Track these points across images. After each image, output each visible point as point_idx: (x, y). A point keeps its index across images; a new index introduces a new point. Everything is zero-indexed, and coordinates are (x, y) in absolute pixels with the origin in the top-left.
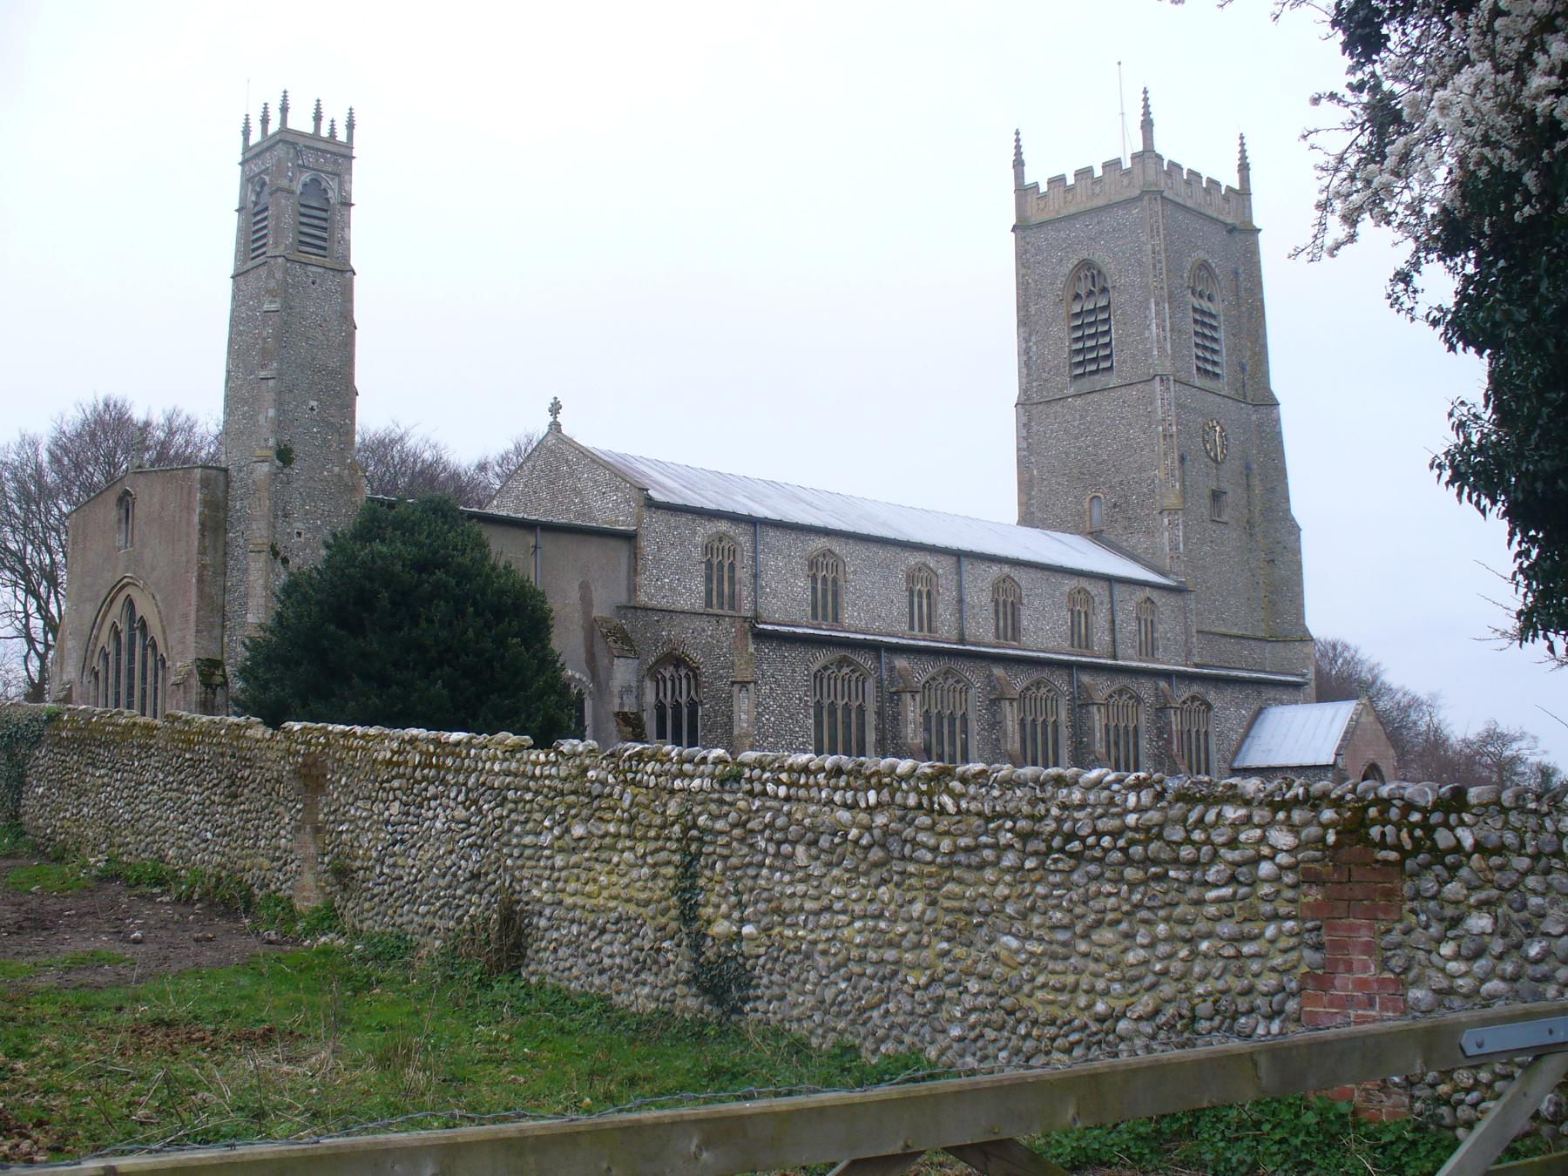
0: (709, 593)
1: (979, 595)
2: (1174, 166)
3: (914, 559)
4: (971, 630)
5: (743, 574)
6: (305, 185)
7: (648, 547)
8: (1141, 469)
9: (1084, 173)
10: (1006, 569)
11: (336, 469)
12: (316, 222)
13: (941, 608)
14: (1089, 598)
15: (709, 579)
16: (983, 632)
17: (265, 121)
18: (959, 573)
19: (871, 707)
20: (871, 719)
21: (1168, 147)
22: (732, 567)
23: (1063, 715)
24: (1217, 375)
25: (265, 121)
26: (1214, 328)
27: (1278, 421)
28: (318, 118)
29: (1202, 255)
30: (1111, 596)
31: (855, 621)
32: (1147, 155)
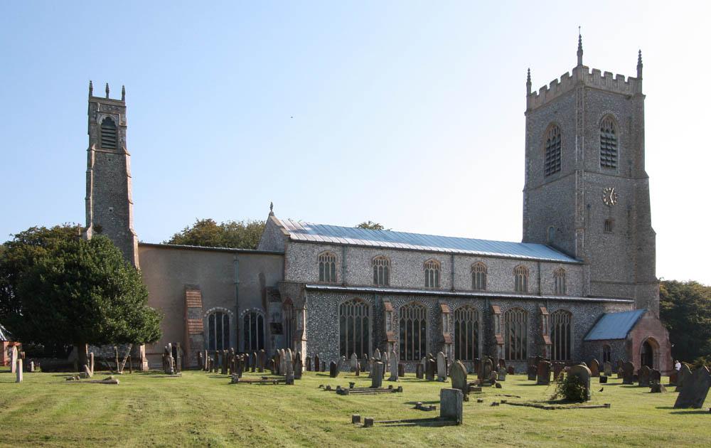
0: (321, 275)
4: (458, 285)
5: (338, 267)
6: (103, 120)
7: (290, 258)
8: (569, 213)
9: (554, 83)
10: (479, 259)
11: (123, 234)
12: (109, 135)
13: (442, 277)
14: (526, 272)
15: (321, 270)
16: (465, 284)
19: (371, 318)
20: (371, 323)
21: (590, 62)
22: (333, 265)
23: (481, 319)
24: (615, 167)
26: (615, 146)
27: (648, 185)
28: (107, 91)
29: (609, 111)
30: (539, 267)
32: (580, 68)
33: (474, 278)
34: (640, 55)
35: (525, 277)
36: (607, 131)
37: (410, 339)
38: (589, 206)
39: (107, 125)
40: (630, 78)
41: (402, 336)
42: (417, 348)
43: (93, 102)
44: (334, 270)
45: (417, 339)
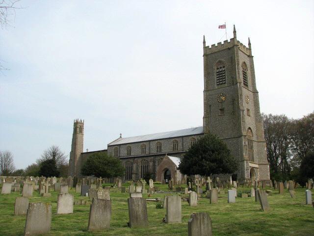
1: (154, 146)
2: (213, 46)
3: (141, 144)
10: (159, 141)
21: (209, 44)
31: (133, 154)
34: (234, 27)
36: (221, 68)
38: (210, 106)
40: (231, 39)
43: (75, 123)
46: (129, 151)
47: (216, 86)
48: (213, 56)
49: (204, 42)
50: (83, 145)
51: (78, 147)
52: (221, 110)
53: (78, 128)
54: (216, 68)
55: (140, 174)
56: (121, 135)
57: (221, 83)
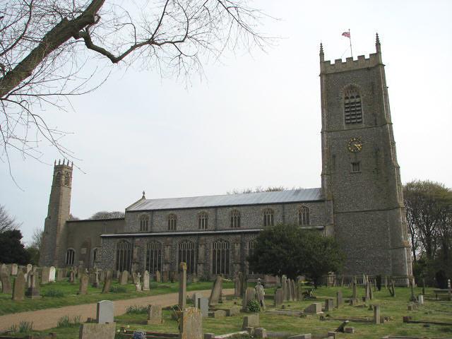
1: (224, 218)
2: (338, 61)
16: (225, 226)
17: (60, 162)
18: (216, 212)
21: (331, 57)
25: (60, 162)
31: (180, 230)
33: (232, 221)
34: (377, 37)
35: (272, 216)
36: (352, 97)
37: (152, 261)
38: (334, 156)
39: (62, 176)
40: (370, 55)
41: (148, 260)
42: (155, 266)
44: (147, 224)
45: (155, 262)
46: (173, 223)
47: (344, 124)
48: (339, 76)
49: (322, 54)
50: (69, 207)
51: (62, 208)
52: (354, 164)
53: (62, 176)
54: (343, 96)
55: (211, 265)
56: (144, 193)
57: (353, 121)
